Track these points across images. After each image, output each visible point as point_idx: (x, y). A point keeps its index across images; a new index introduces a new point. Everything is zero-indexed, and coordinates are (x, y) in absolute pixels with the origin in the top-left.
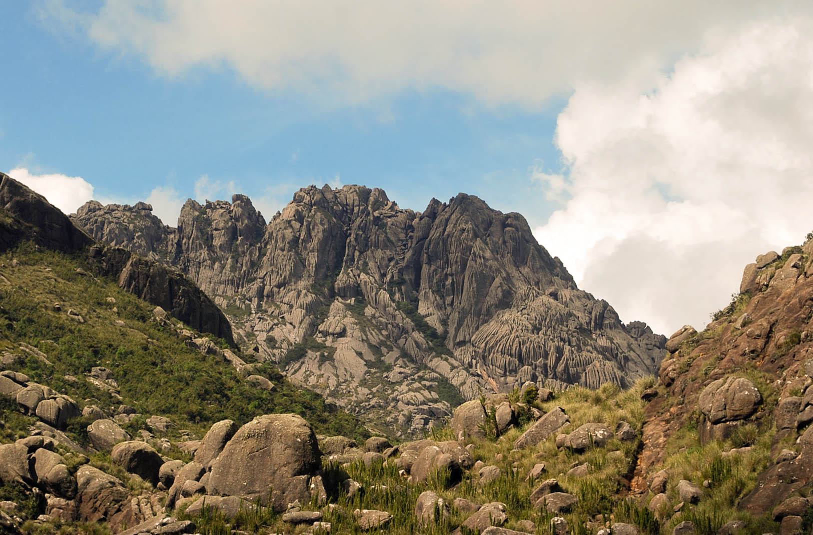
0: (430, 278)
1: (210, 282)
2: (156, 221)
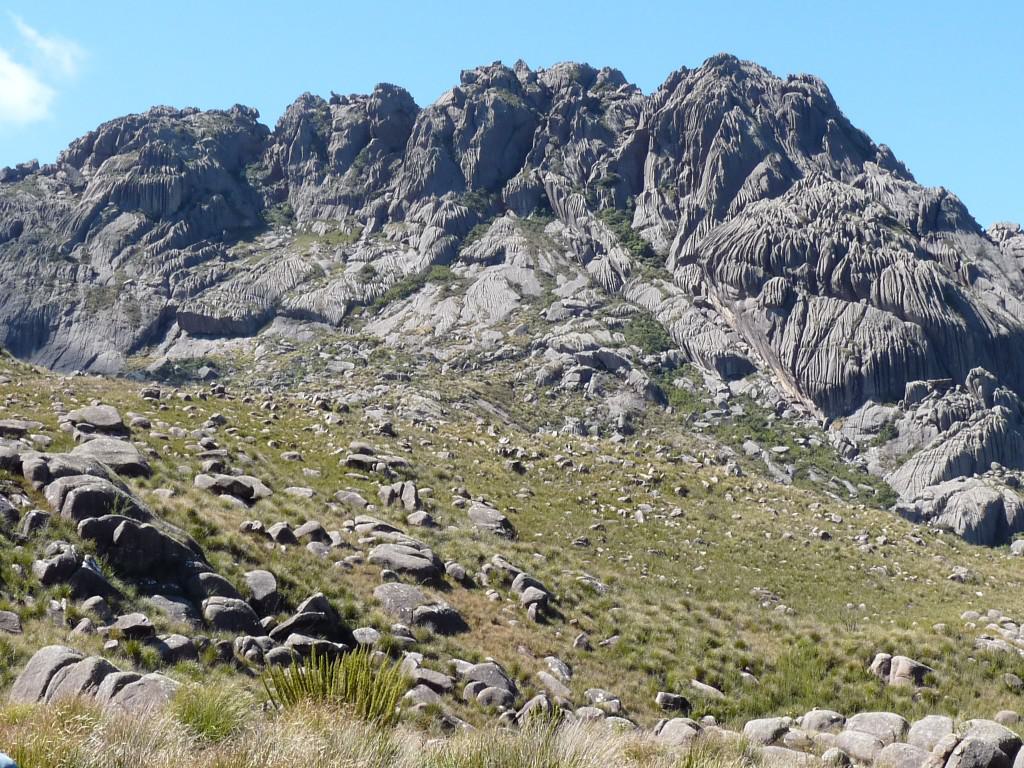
0: (658, 173)
1: (312, 203)
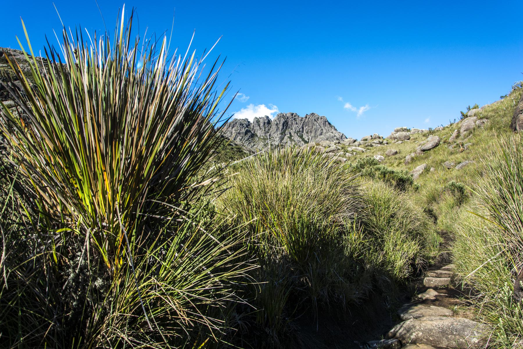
2: (249, 122)
